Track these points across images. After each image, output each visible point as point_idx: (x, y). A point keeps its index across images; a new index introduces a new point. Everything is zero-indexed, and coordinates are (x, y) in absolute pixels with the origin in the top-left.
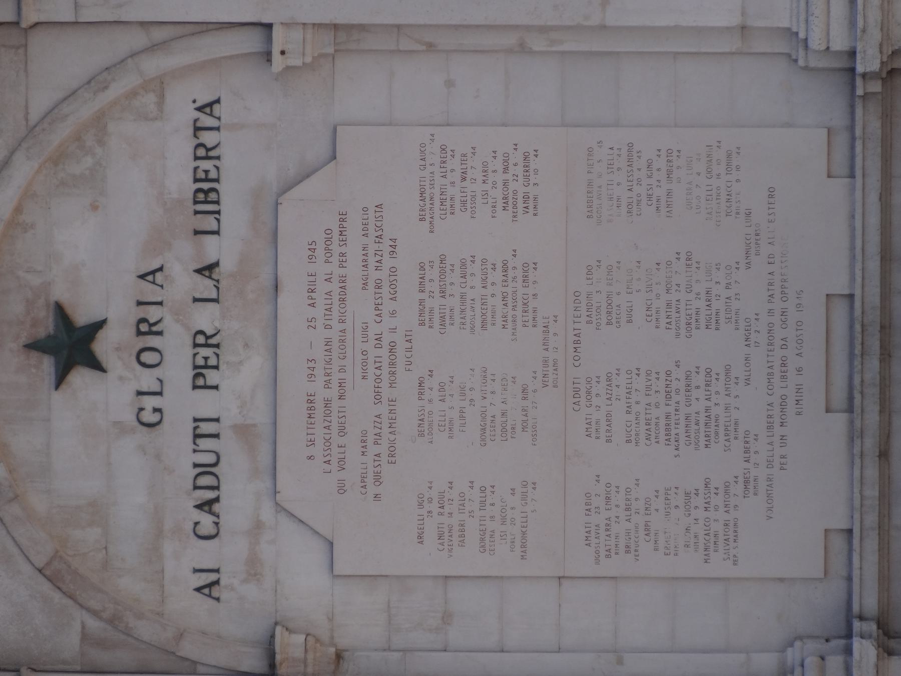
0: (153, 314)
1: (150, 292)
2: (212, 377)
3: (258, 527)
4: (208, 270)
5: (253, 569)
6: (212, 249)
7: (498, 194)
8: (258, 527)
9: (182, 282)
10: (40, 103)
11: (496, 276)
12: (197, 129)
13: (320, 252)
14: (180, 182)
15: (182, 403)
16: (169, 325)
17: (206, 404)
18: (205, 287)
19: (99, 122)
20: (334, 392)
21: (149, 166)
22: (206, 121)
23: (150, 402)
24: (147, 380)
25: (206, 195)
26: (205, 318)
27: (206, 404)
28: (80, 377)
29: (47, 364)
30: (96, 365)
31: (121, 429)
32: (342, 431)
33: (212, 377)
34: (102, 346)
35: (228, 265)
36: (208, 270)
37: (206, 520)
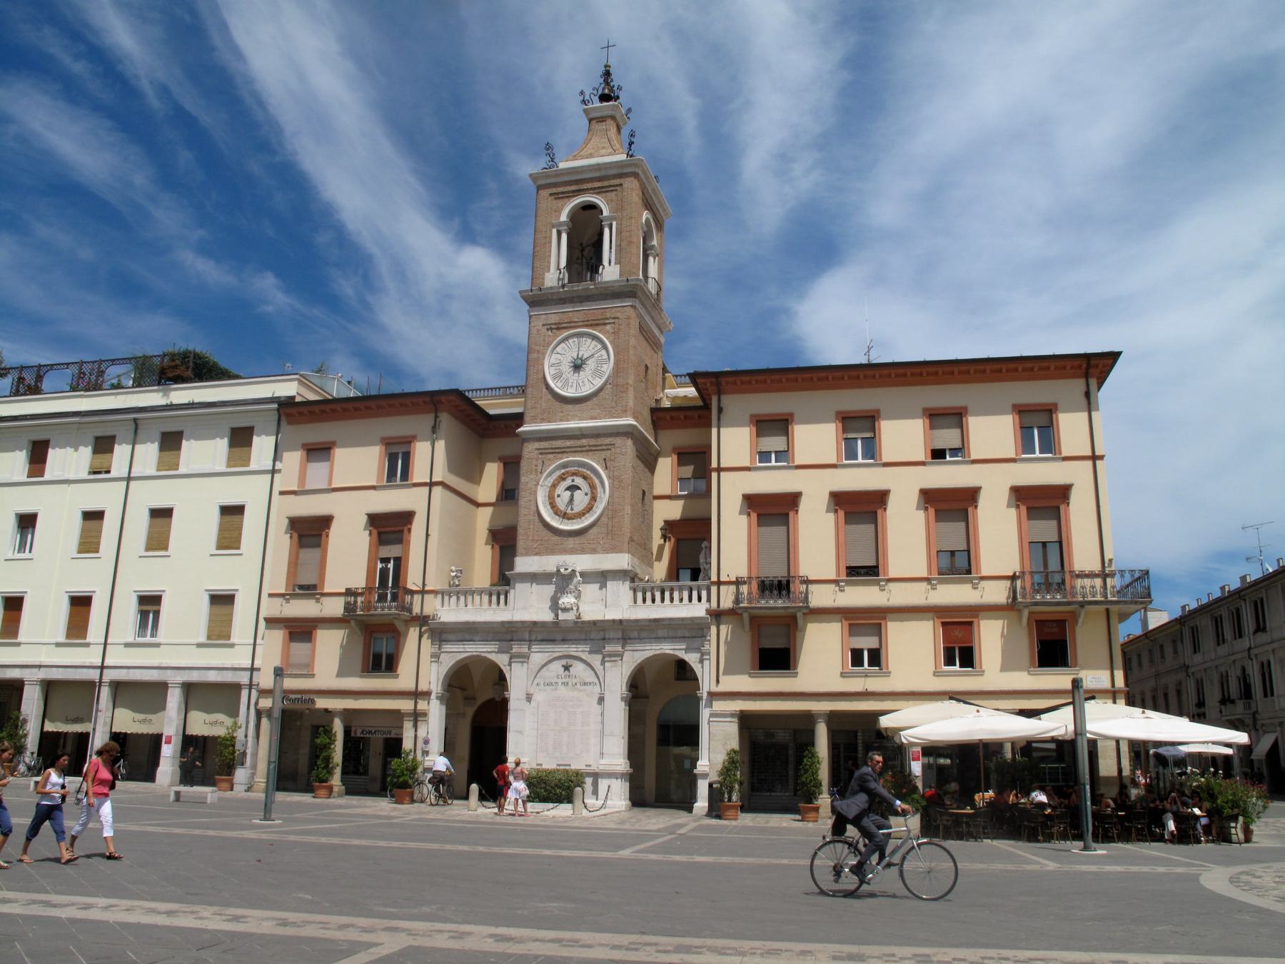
14: (587, 680)
15: (560, 681)
21: (588, 676)
25: (585, 684)
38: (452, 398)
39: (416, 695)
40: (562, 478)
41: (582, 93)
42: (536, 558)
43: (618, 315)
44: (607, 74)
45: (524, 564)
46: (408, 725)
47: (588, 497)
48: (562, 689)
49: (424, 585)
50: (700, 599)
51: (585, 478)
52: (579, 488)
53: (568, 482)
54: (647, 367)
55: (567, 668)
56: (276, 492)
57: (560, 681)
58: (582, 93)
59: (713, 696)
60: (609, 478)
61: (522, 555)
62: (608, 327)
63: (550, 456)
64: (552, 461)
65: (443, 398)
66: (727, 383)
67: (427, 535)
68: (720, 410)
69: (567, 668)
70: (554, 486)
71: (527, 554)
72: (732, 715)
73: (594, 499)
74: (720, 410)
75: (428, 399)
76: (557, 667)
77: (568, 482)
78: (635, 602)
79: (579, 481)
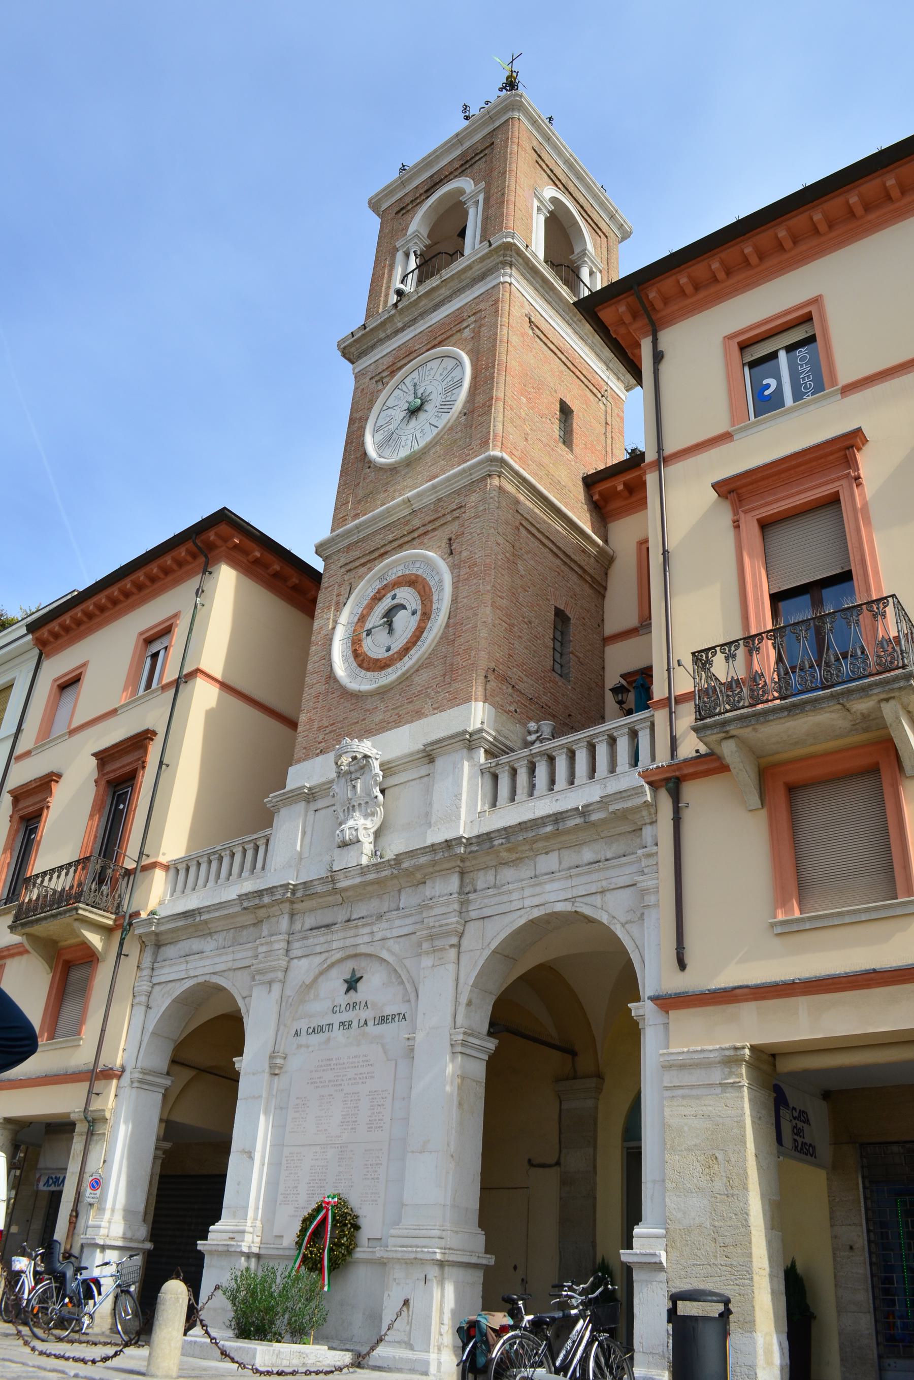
0: (357, 1007)
1: (363, 1004)
2: (342, 1027)
3: (308, 1046)
4: (366, 1023)
5: (299, 1046)
6: (370, 1023)
7: (373, 1118)
8: (308, 1046)
9: (364, 1014)
10: (407, 962)
11: (354, 1119)
12: (399, 1014)
13: (365, 1058)
14: (389, 1011)
16: (355, 1012)
17: (336, 1026)
18: (362, 1023)
19: (402, 983)
20: (332, 1067)
22: (401, 1016)
23: (338, 1009)
24: (343, 1007)
25: (383, 1020)
26: (355, 1024)
27: (336, 1026)
28: (345, 986)
29: (348, 976)
30: (348, 991)
31: (333, 1001)
32: (324, 1070)
33: (342, 1027)
34: (352, 992)
35: (366, 1029)
36: (366, 1023)
37: (310, 1031)
38: (223, 528)
39: (98, 1075)
40: (377, 598)
41: (466, 107)
42: (321, 758)
43: (482, 306)
44: (511, 84)
45: (303, 775)
46: (77, 1145)
47: (418, 616)
48: (338, 1034)
49: (141, 853)
50: (635, 761)
51: (412, 582)
52: (404, 607)
53: (386, 603)
54: (565, 411)
55: (352, 984)
56: (13, 760)
57: (336, 1019)
58: (466, 107)
59: (668, 1003)
60: (453, 567)
61: (299, 761)
62: (467, 333)
63: (362, 570)
64: (361, 578)
65: (212, 536)
66: (666, 301)
67: (161, 763)
68: (658, 357)
69: (352, 984)
70: (362, 619)
71: (307, 758)
72: (730, 1060)
73: (426, 616)
74: (658, 357)
75: (190, 545)
76: (335, 984)
77: (386, 603)
78: (494, 804)
79: (406, 595)
